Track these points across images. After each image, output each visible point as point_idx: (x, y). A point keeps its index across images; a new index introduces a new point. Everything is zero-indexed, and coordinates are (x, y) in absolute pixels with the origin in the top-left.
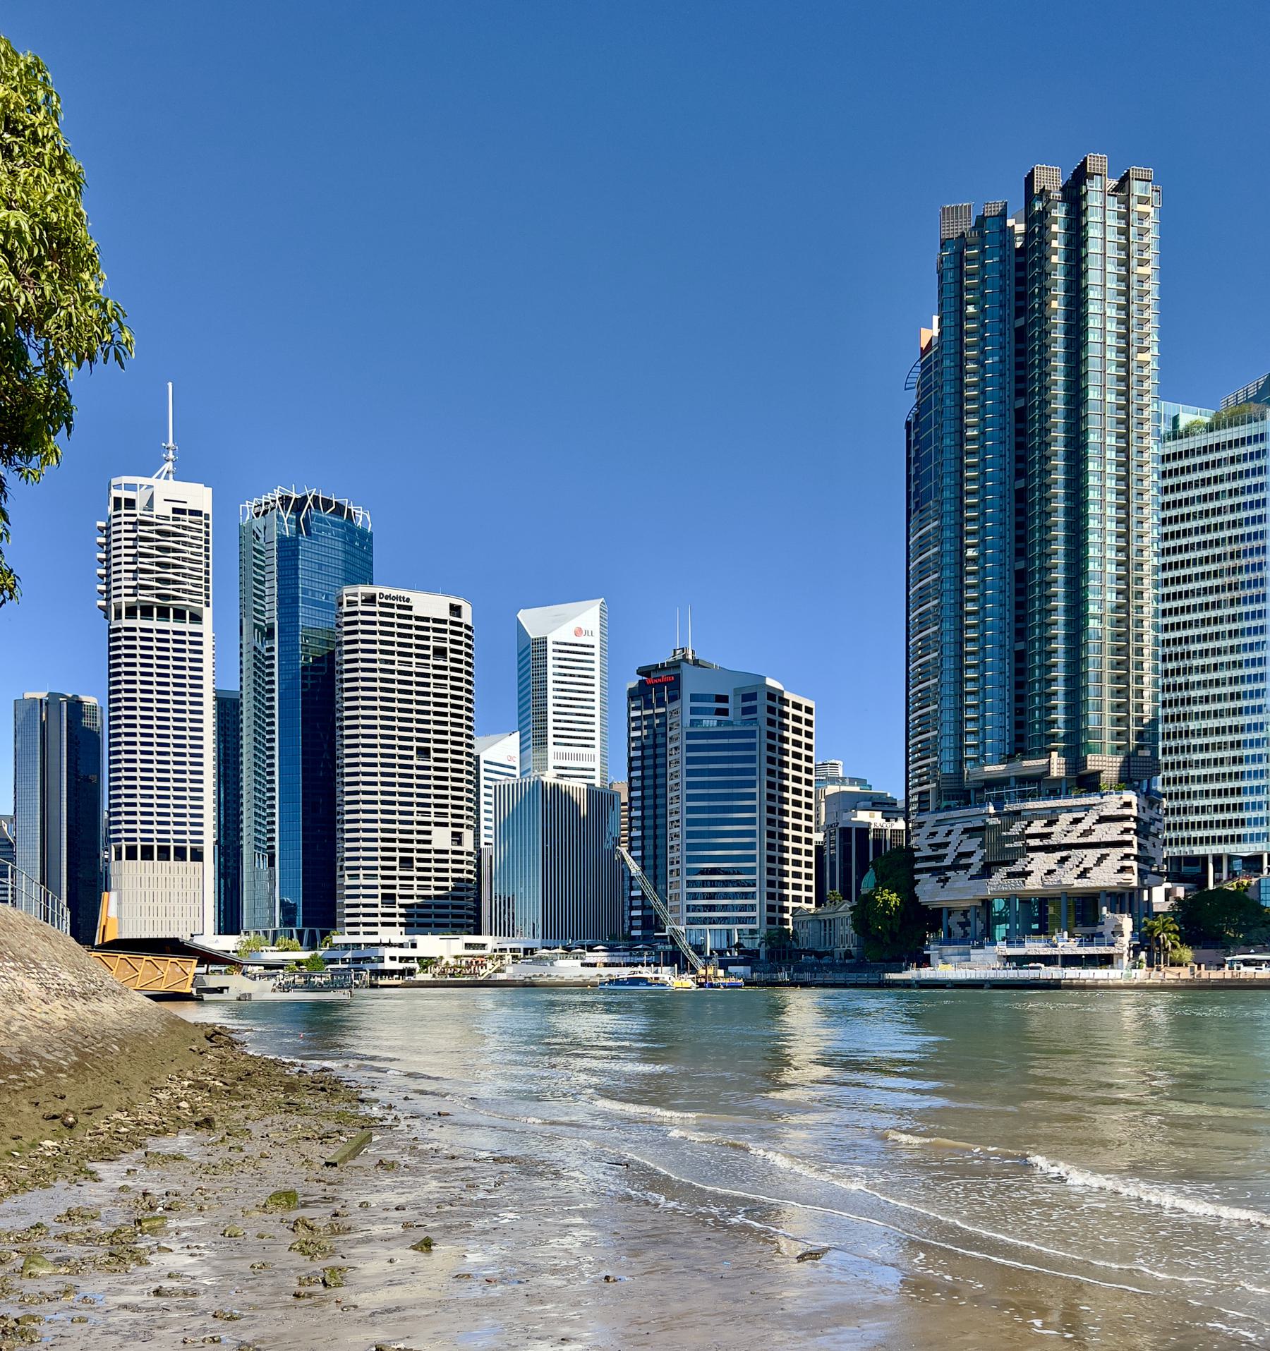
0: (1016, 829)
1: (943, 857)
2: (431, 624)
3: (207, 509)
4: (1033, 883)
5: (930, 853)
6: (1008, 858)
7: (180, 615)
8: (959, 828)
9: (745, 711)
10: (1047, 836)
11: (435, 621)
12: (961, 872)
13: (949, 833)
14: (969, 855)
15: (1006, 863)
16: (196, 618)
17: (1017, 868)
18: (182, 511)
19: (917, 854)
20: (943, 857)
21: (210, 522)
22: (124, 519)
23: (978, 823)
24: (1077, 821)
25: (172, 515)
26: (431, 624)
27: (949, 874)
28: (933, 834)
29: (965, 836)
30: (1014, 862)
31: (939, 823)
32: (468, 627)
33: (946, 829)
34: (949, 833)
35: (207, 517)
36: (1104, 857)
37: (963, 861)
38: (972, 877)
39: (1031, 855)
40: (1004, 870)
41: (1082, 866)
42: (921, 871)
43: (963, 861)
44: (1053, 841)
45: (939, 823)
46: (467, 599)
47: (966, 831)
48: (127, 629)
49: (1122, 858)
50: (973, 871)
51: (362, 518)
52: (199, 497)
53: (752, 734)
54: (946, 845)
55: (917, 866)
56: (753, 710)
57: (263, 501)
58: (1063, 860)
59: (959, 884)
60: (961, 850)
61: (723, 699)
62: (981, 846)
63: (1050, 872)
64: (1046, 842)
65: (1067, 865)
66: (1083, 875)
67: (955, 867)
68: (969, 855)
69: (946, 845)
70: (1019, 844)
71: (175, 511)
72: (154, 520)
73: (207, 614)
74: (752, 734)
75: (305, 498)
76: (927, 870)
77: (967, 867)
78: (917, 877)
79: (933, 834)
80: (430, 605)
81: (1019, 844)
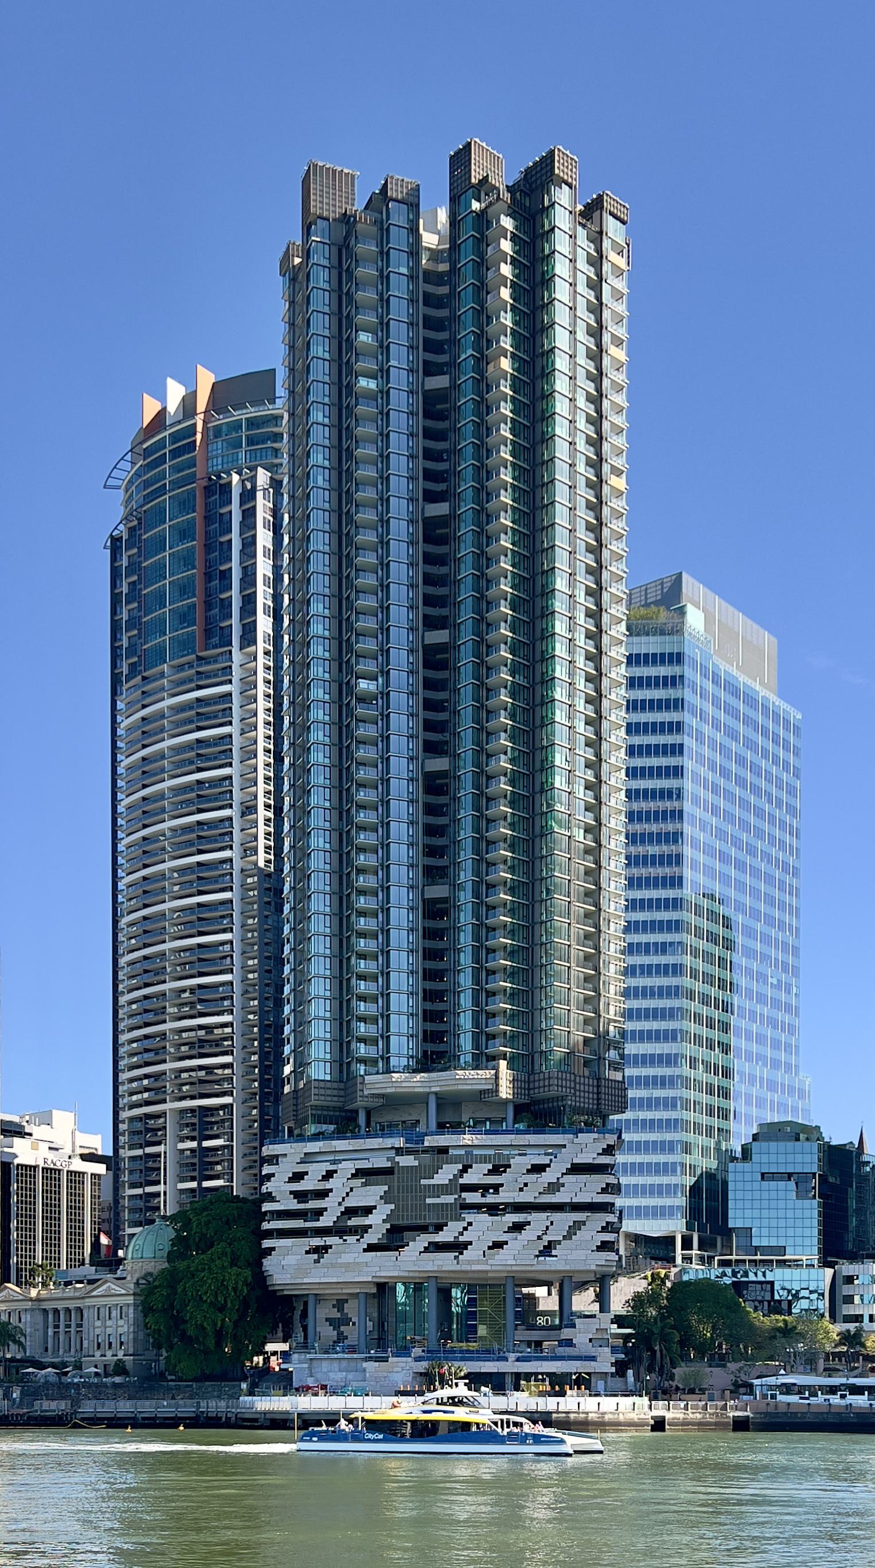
0: (445, 1175)
1: (319, 1213)
4: (473, 1260)
5: (293, 1205)
6: (431, 1219)
8: (348, 1167)
10: (496, 1188)
12: (351, 1239)
13: (329, 1175)
14: (368, 1210)
15: (423, 1229)
17: (445, 1236)
19: (266, 1207)
20: (319, 1213)
23: (381, 1162)
24: (538, 1169)
27: (330, 1240)
28: (298, 1177)
29: (358, 1182)
30: (439, 1228)
31: (308, 1158)
33: (325, 1167)
34: (329, 1175)
36: (577, 1226)
37: (354, 1222)
38: (371, 1248)
39: (469, 1217)
40: (423, 1240)
41: (546, 1238)
42: (270, 1234)
43: (354, 1222)
44: (504, 1196)
45: (308, 1158)
47: (359, 1173)
49: (604, 1229)
50: (372, 1237)
54: (323, 1194)
55: (266, 1226)
58: (517, 1227)
59: (347, 1258)
60: (351, 1202)
62: (386, 1198)
63: (498, 1245)
64: (491, 1199)
65: (529, 1234)
66: (547, 1250)
67: (339, 1230)
68: (368, 1210)
69: (323, 1194)
70: (450, 1199)
76: (283, 1233)
77: (365, 1229)
78: (267, 1243)
79: (298, 1177)
81: (450, 1199)
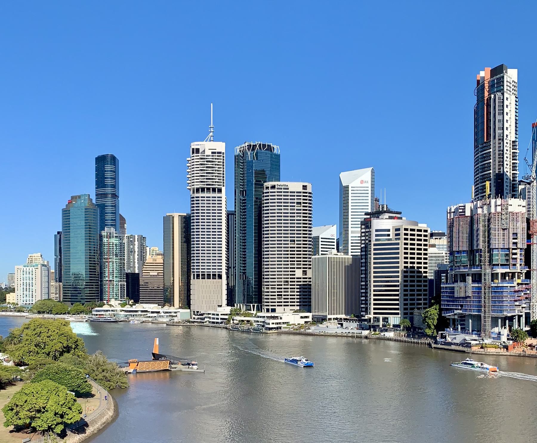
2: (296, 194)
3: (223, 150)
7: (214, 190)
9: (397, 235)
11: (297, 192)
16: (220, 191)
18: (215, 153)
21: (225, 155)
22: (195, 157)
25: (211, 155)
26: (296, 194)
32: (310, 193)
35: (223, 153)
46: (309, 182)
48: (196, 197)
51: (277, 149)
52: (221, 147)
53: (398, 244)
56: (399, 235)
57: (242, 146)
61: (389, 230)
71: (212, 153)
72: (205, 157)
73: (224, 189)
74: (398, 244)
75: (256, 145)
80: (296, 186)
